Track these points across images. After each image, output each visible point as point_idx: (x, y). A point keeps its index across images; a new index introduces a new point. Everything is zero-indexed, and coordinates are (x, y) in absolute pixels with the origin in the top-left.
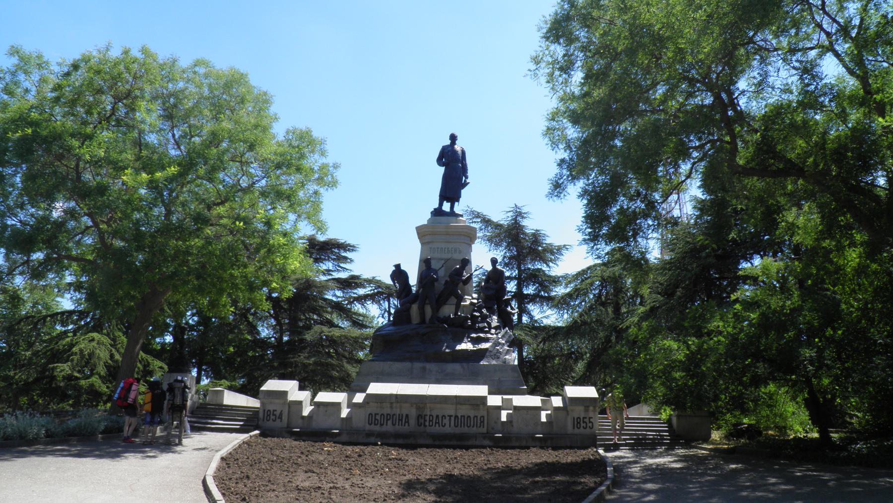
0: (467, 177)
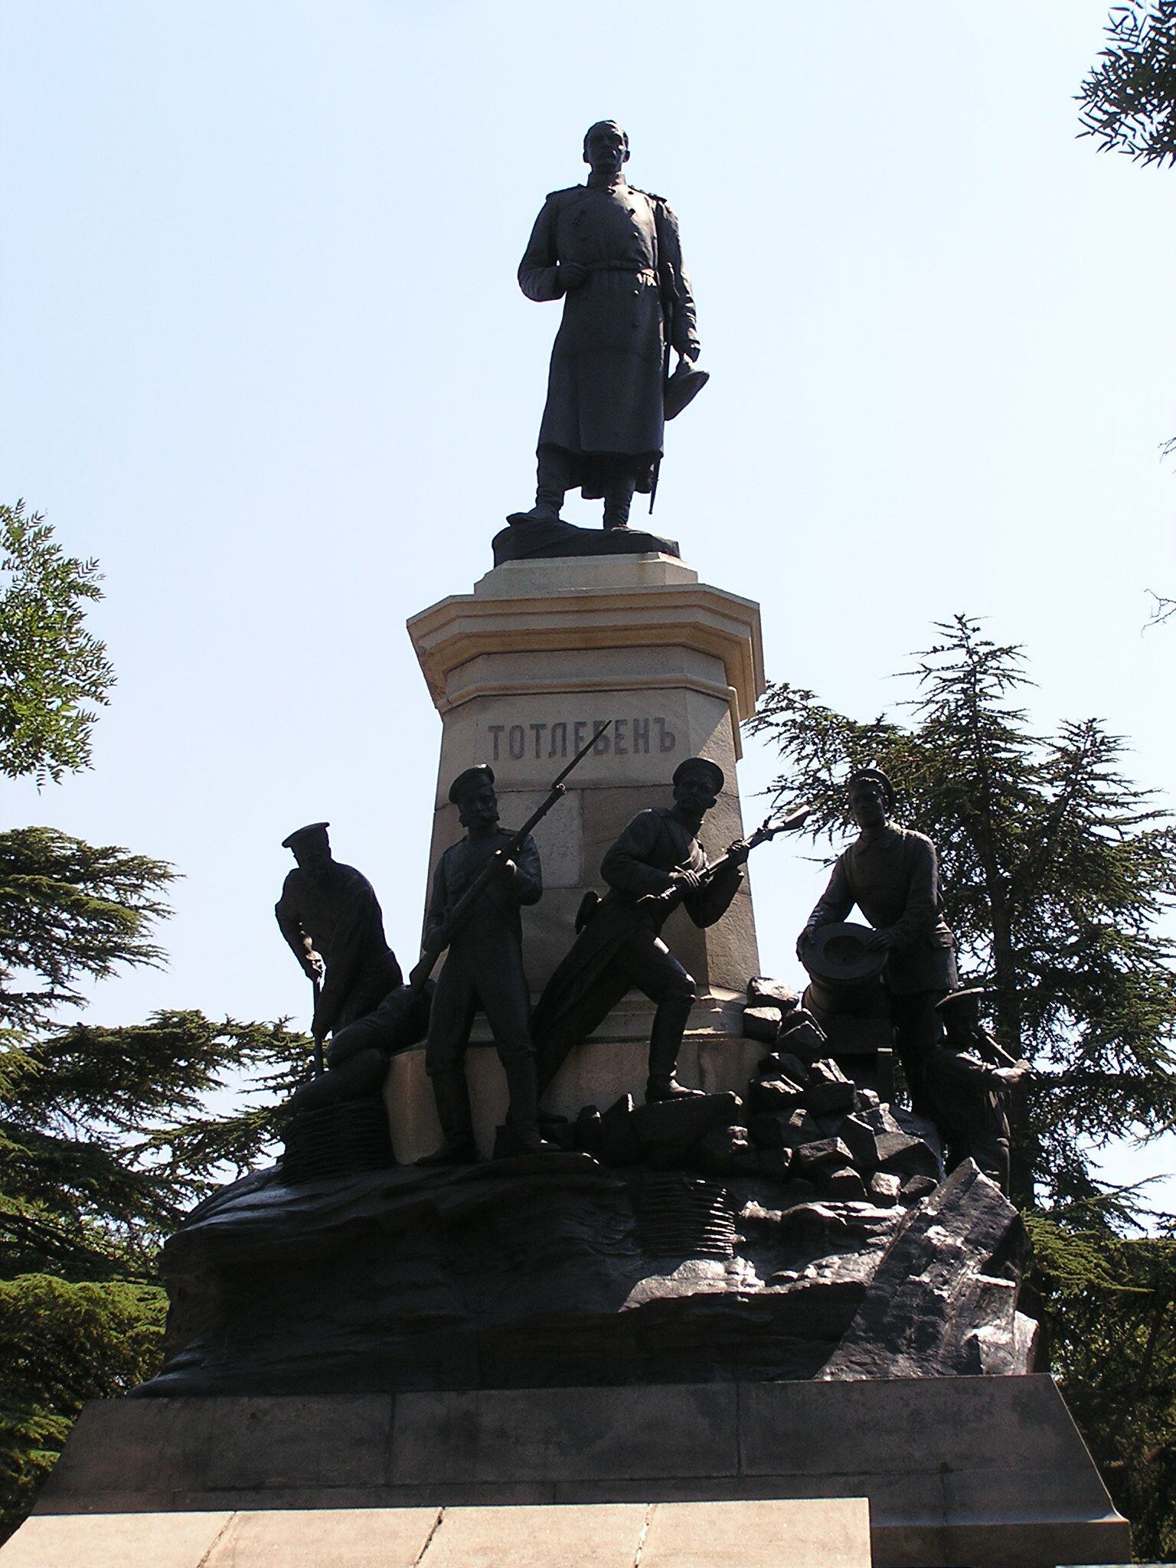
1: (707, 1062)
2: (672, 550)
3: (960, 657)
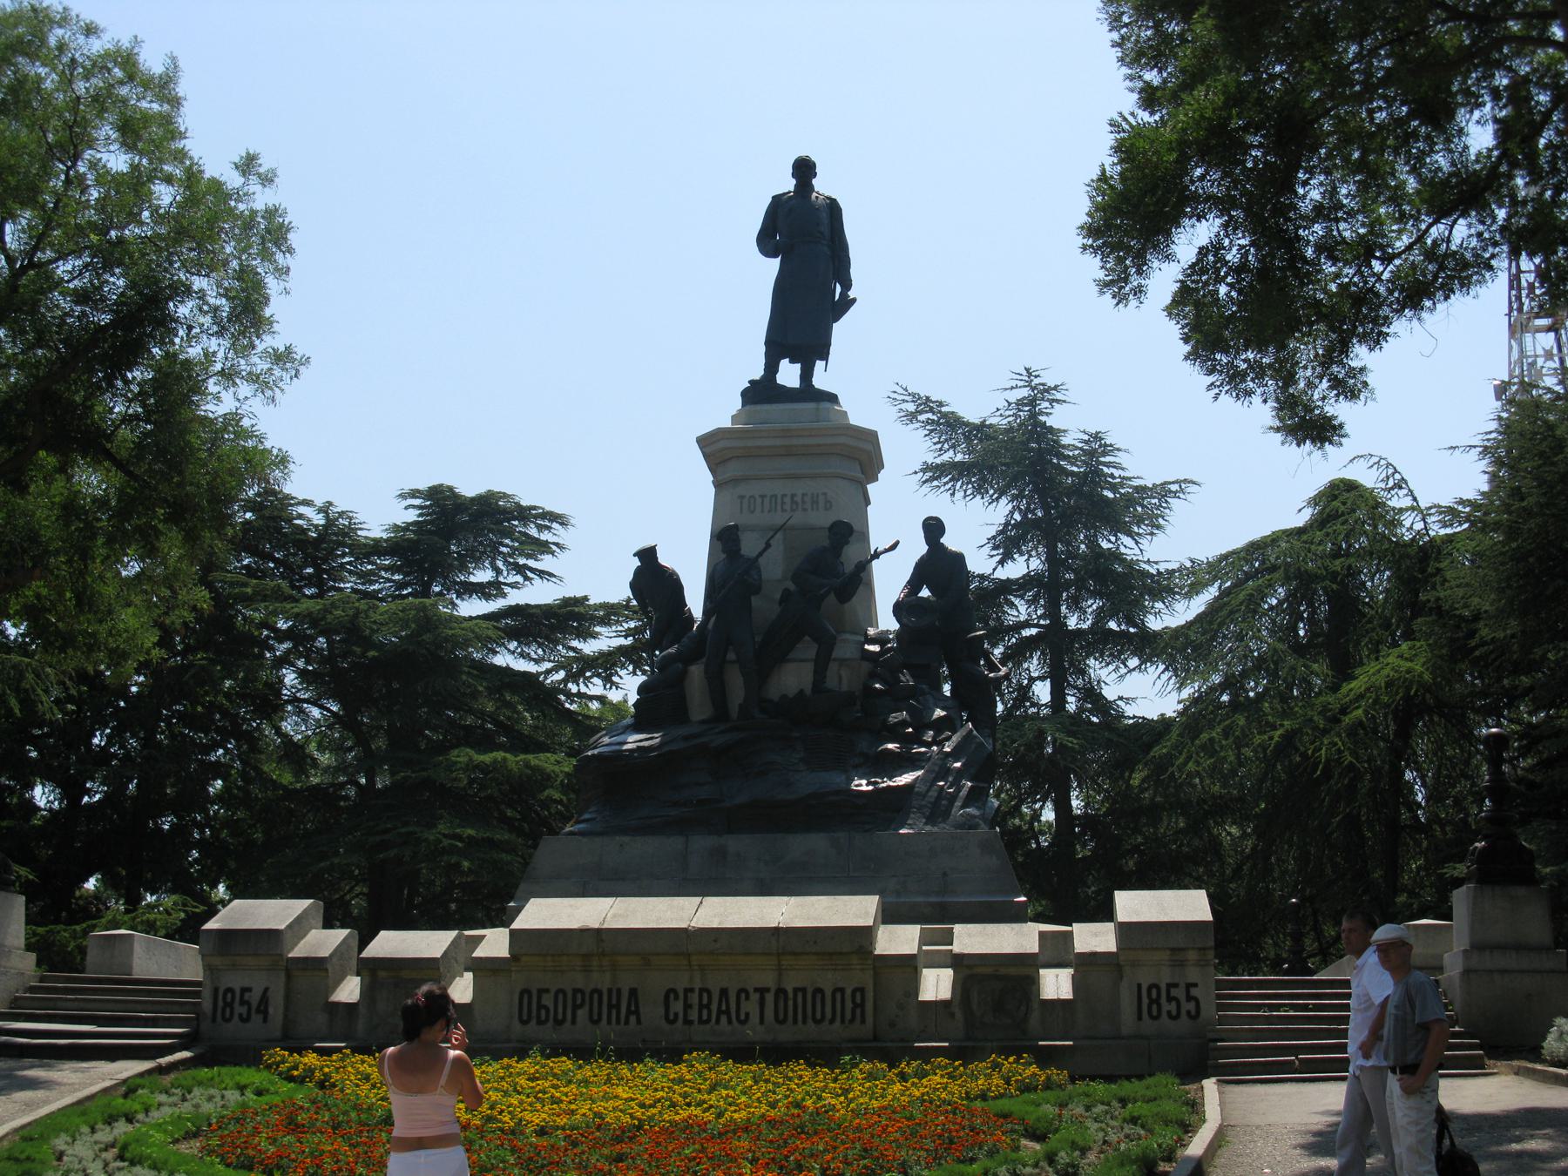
0: (847, 285)
1: (843, 673)
3: (1025, 392)
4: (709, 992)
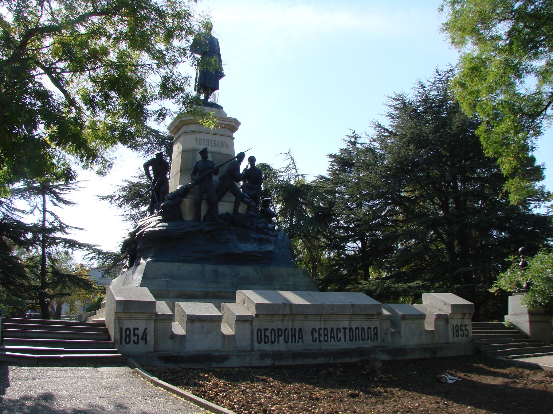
2: (222, 108)
4: (327, 330)
